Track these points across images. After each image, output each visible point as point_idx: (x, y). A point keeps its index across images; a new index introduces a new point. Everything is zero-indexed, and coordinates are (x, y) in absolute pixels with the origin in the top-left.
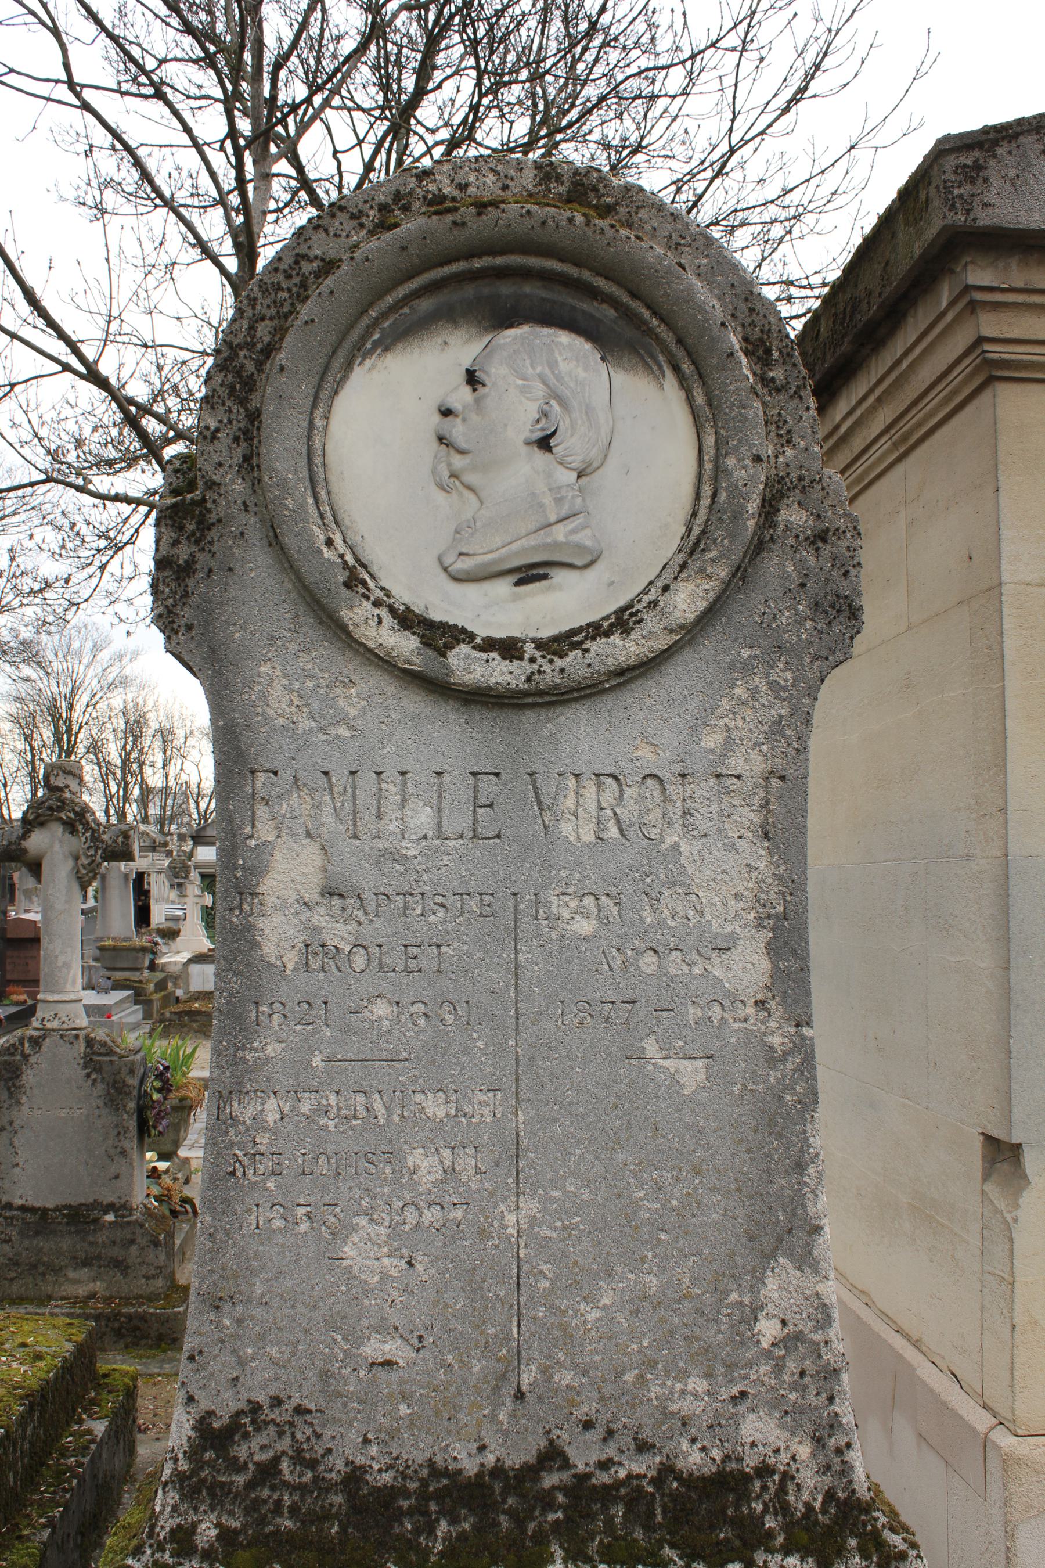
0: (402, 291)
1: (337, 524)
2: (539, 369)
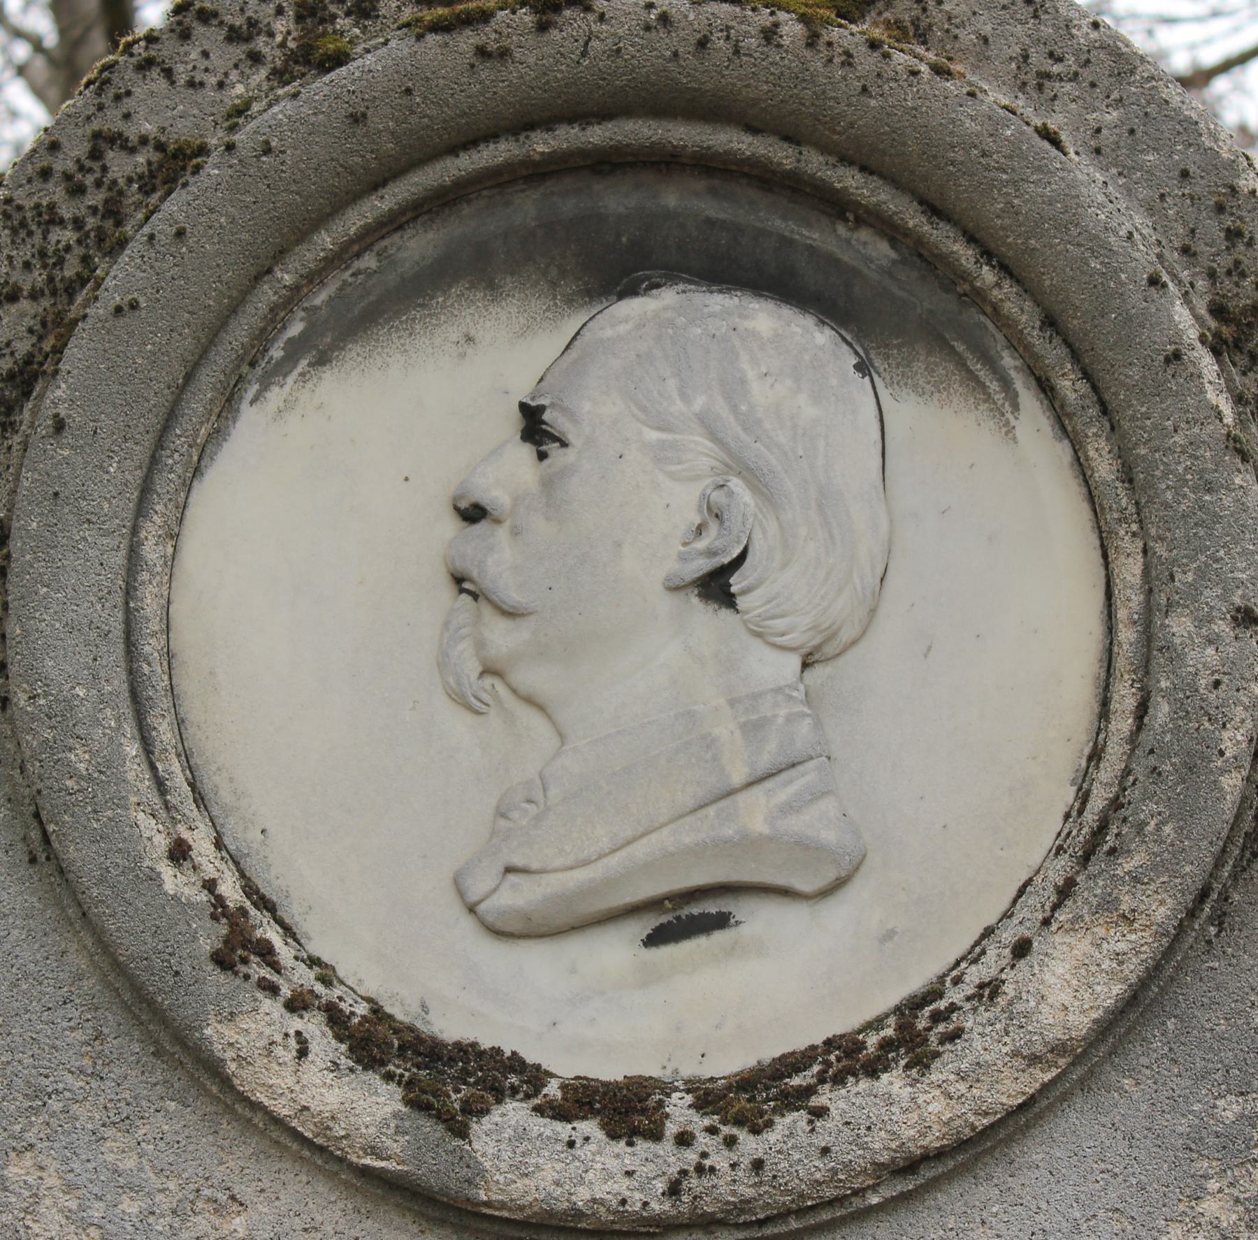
0: (355, 219)
1: (200, 799)
2: (699, 402)
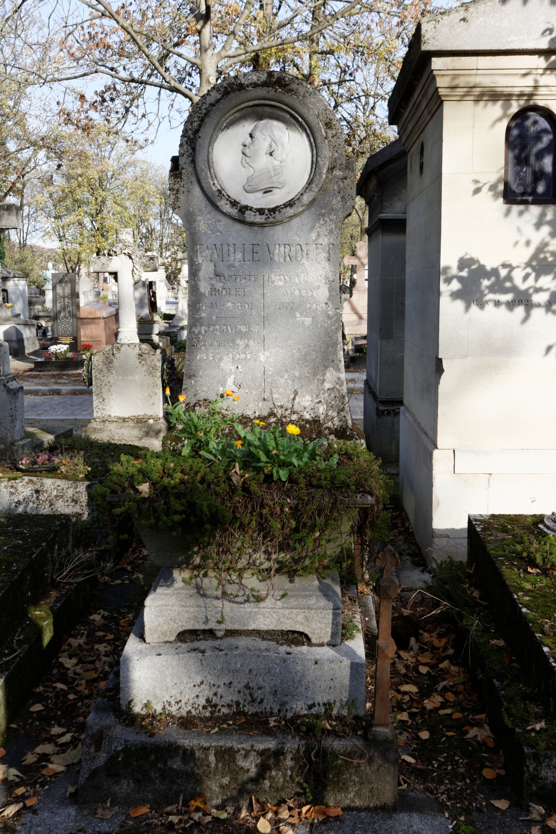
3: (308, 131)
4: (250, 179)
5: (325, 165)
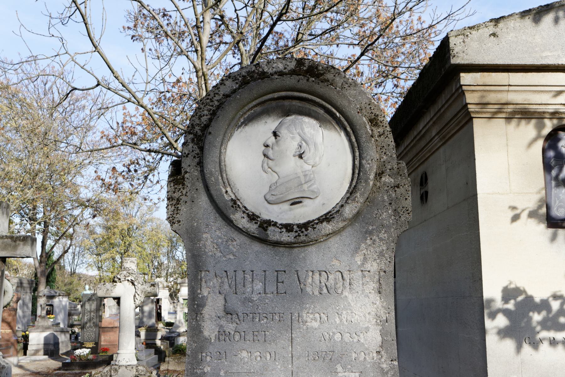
1: (229, 185)
2: (298, 131)
3: (349, 129)
4: (273, 188)
5: (371, 168)
